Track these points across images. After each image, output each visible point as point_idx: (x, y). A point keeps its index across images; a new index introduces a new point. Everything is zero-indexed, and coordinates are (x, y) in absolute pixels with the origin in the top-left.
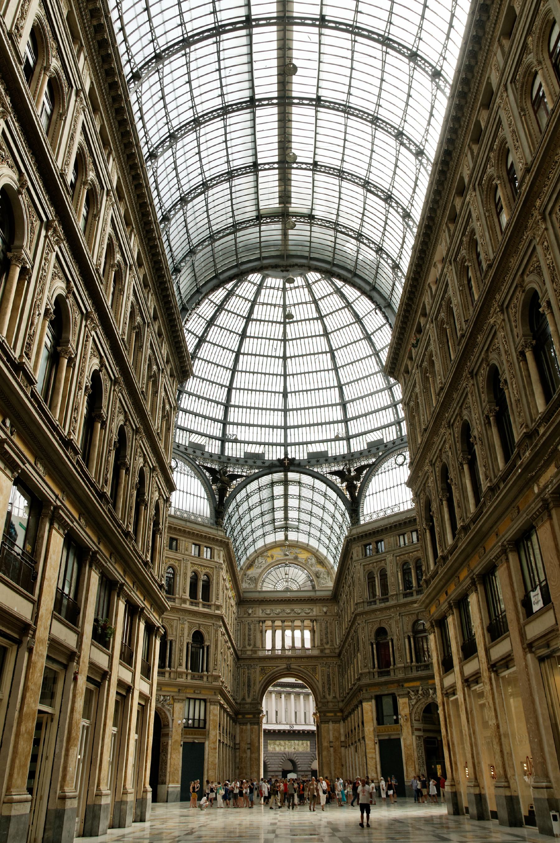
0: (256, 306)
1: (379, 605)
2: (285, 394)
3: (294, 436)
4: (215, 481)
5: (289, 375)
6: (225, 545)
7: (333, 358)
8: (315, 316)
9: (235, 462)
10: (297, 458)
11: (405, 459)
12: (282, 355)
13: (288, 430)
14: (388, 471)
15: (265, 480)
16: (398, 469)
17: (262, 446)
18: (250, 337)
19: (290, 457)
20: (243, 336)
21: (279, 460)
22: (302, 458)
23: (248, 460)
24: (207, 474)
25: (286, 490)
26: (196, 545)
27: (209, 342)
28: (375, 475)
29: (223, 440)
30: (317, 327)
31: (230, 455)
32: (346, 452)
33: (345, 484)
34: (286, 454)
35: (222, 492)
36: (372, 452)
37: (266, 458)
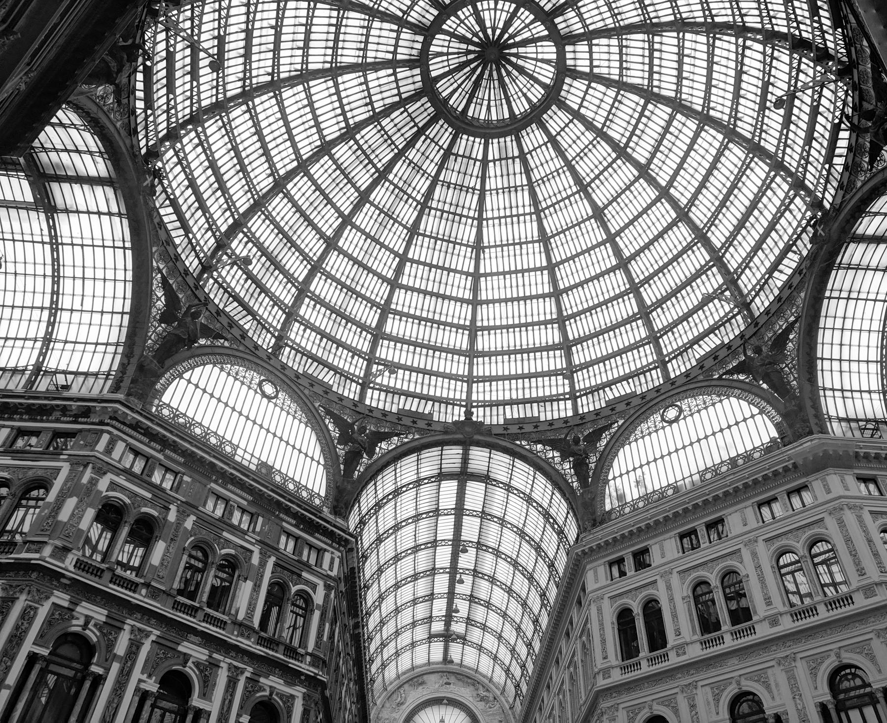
2: (473, 330)
4: (343, 440)
6: (346, 544)
9: (380, 416)
10: (488, 421)
11: (681, 411)
12: (472, 270)
13: (475, 385)
15: (429, 462)
16: (668, 429)
17: (430, 403)
21: (455, 423)
22: (495, 422)
23: (404, 418)
28: (623, 446)
29: (365, 384)
31: (374, 404)
32: (570, 413)
33: (567, 466)
34: (469, 414)
35: (352, 459)
36: (618, 409)
37: (436, 418)
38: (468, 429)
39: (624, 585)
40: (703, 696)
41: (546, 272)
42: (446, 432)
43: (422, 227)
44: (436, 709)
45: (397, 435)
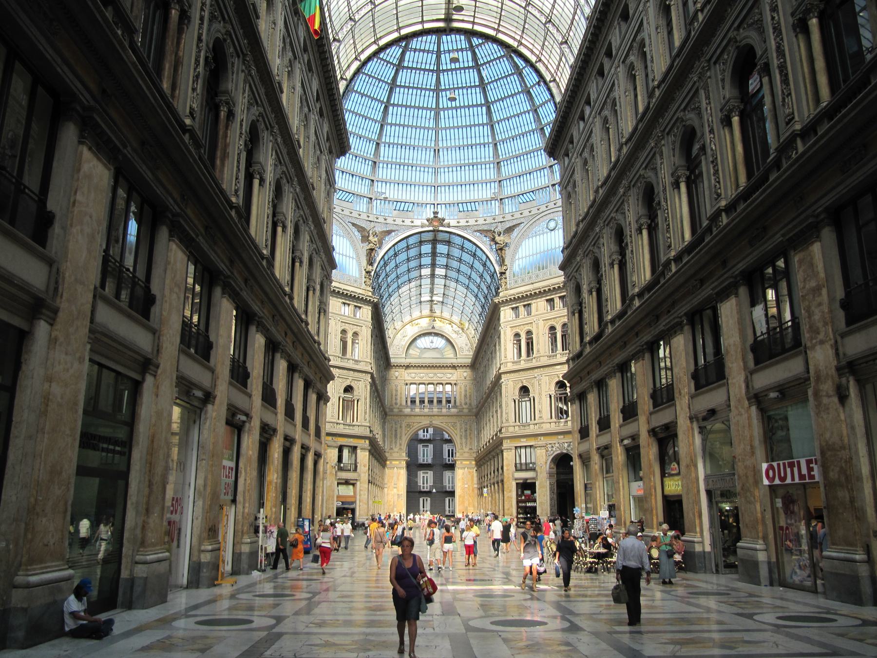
0: (408, 53)
1: (523, 365)
2: (436, 152)
3: (445, 196)
5: (442, 129)
7: (489, 112)
8: (471, 65)
14: (539, 235)
18: (400, 86)
19: (439, 216)
20: (393, 85)
24: (357, 233)
25: (434, 248)
26: (344, 304)
27: (356, 92)
30: (472, 77)
34: (435, 213)
38: (436, 224)
39: (519, 322)
40: (545, 379)
41: (484, 108)
42: (422, 227)
43: (399, 80)
44: (427, 338)
45: (394, 231)
